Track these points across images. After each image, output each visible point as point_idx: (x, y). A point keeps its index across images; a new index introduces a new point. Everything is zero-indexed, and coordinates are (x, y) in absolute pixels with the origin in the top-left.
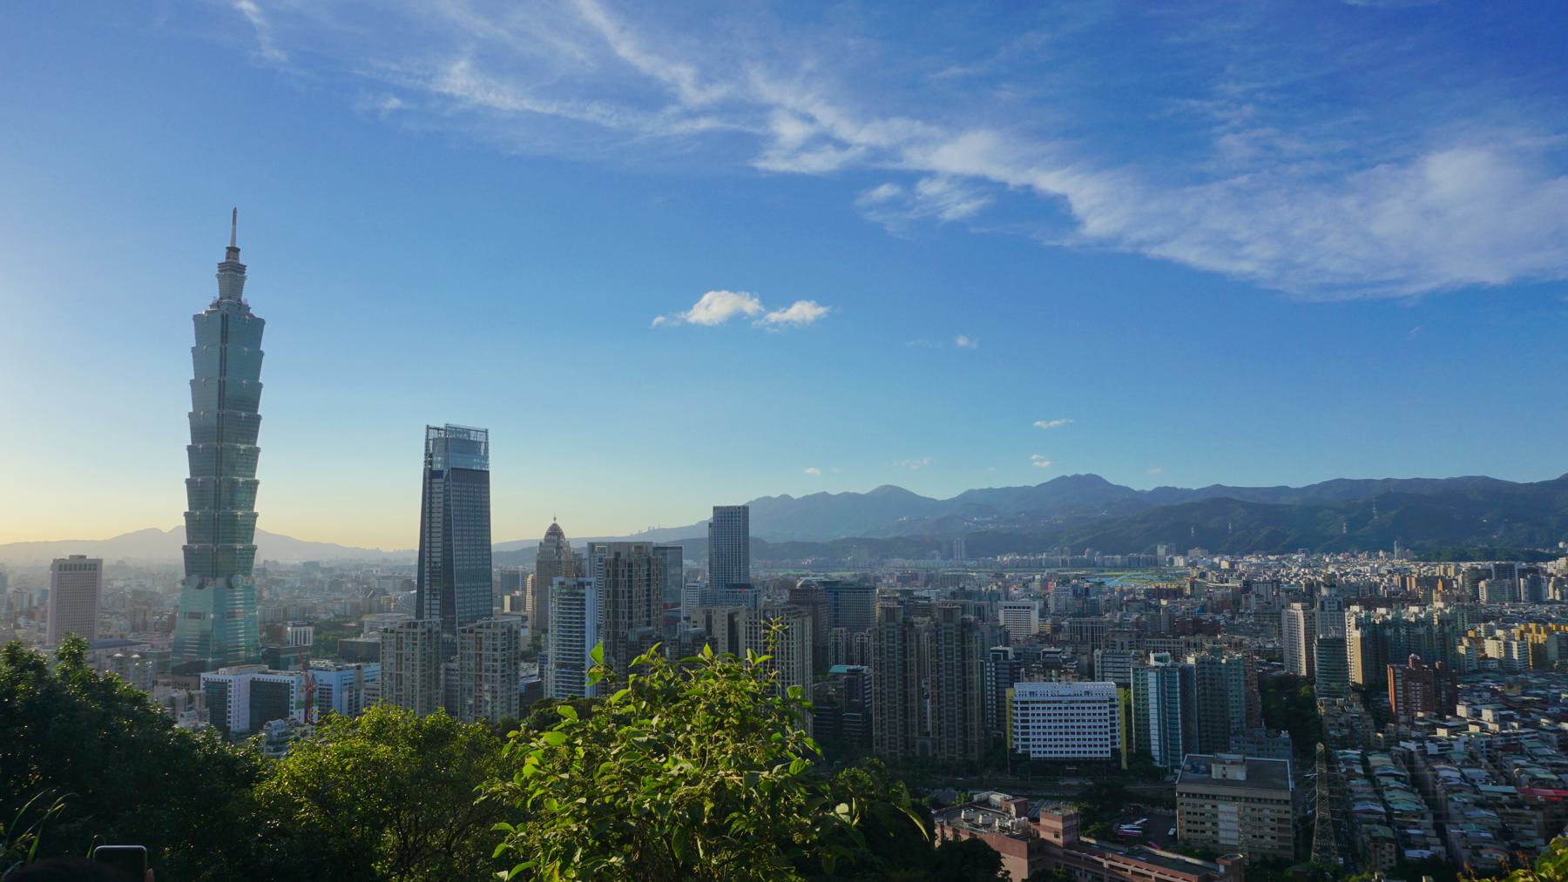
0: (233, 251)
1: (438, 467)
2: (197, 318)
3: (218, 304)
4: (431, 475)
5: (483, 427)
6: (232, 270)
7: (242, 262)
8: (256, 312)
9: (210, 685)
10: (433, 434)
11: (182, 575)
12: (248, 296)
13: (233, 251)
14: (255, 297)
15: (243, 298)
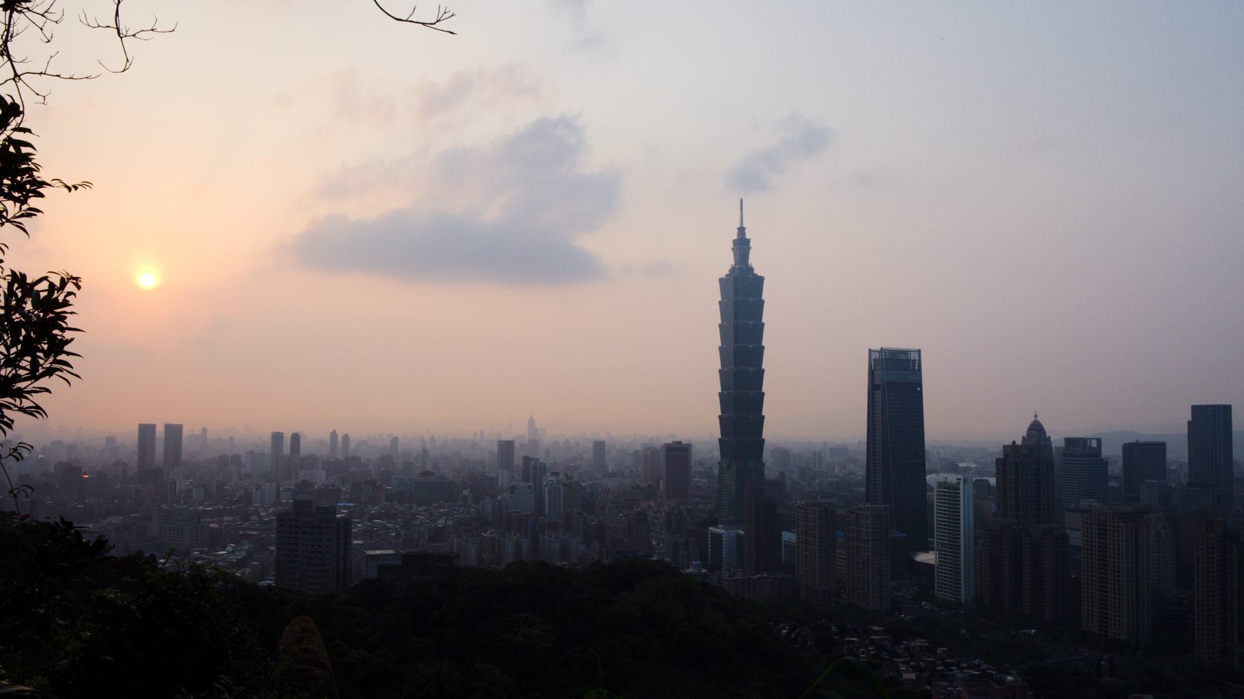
0: (741, 230)
1: (877, 382)
2: (721, 280)
3: (732, 270)
4: (873, 388)
5: (917, 348)
6: (742, 246)
7: (748, 237)
8: (758, 271)
9: (713, 534)
10: (876, 356)
11: (719, 459)
12: (754, 260)
13: (741, 230)
14: (758, 262)
15: (750, 261)
